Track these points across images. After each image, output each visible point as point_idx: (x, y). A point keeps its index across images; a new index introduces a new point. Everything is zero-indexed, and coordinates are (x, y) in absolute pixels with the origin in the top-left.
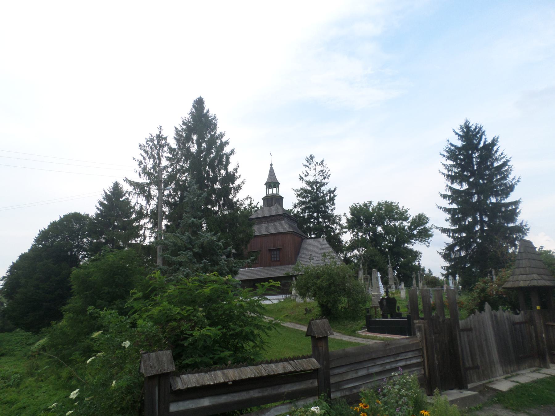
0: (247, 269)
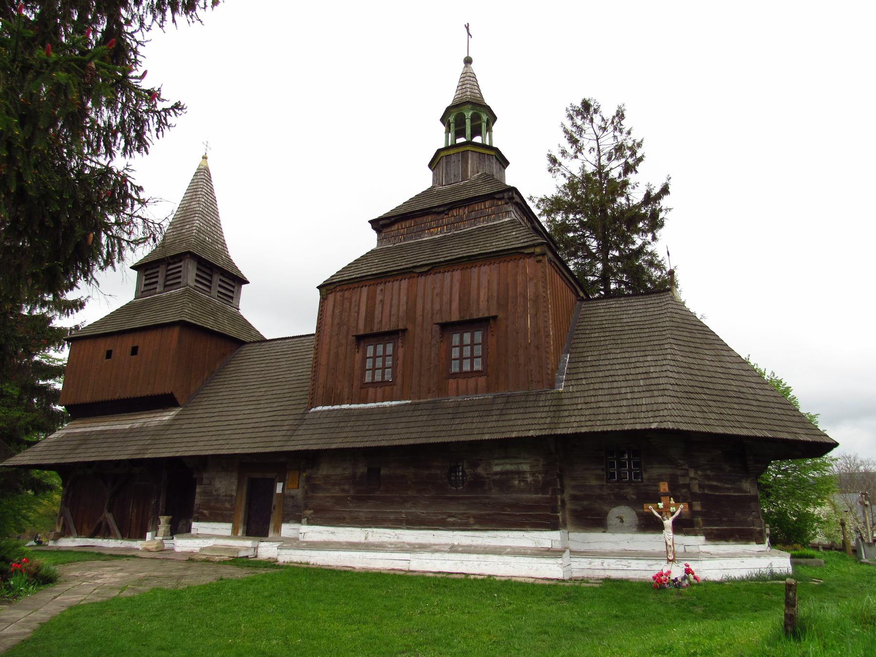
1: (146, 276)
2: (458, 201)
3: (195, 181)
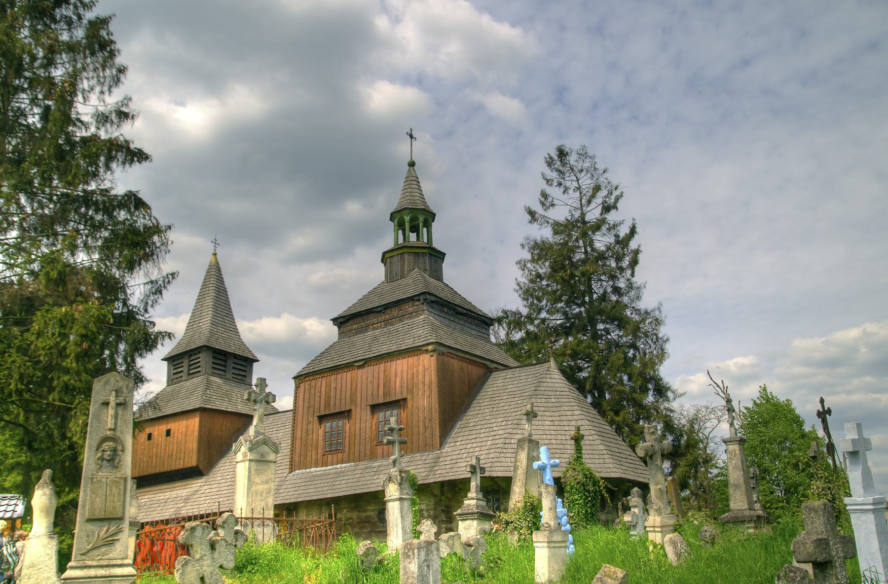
0: (313, 469)
1: (174, 366)
2: (389, 303)
3: (208, 277)
